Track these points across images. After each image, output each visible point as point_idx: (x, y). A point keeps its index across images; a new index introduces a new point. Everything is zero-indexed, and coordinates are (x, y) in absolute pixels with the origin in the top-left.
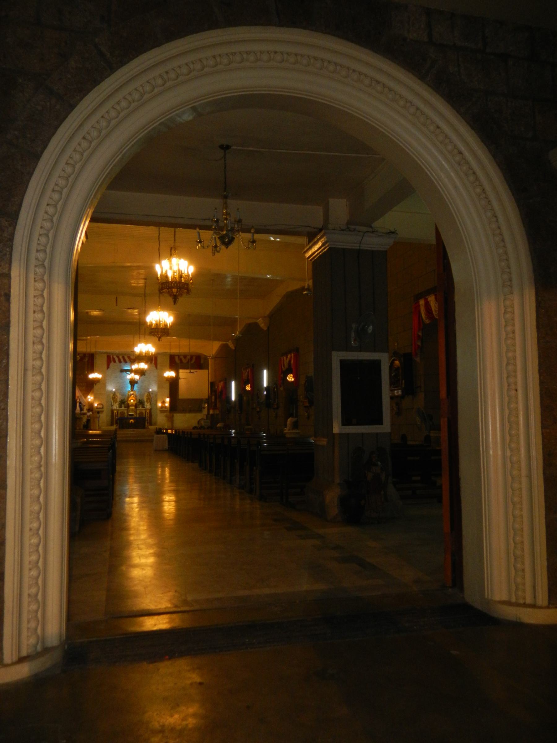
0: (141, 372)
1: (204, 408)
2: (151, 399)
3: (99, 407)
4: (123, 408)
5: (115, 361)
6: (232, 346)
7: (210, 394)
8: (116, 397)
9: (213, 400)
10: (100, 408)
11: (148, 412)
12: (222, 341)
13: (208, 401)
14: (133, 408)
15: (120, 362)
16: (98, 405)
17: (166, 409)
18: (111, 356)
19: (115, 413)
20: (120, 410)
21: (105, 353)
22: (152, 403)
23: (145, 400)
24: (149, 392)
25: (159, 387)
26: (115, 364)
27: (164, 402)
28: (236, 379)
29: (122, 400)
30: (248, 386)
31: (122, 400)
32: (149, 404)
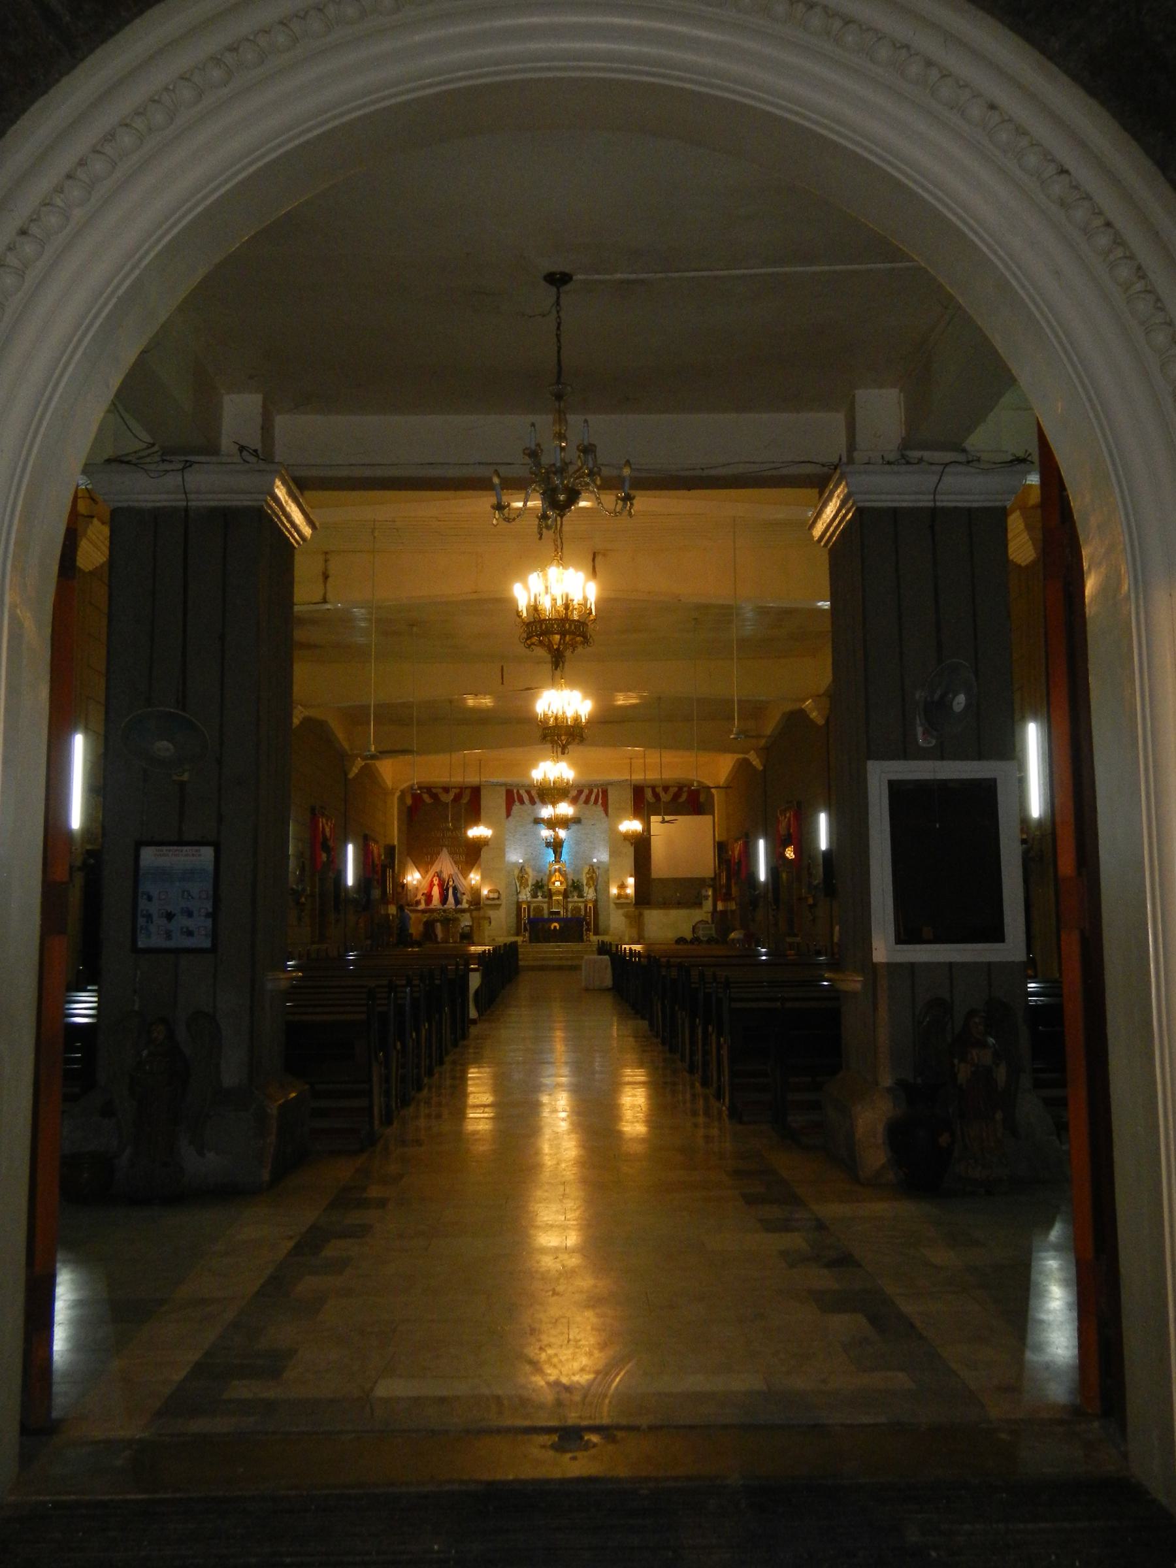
0: (564, 822)
1: (707, 897)
2: (597, 879)
3: (492, 896)
5: (522, 802)
6: (756, 762)
7: (717, 869)
8: (526, 876)
9: (724, 881)
12: (738, 753)
13: (714, 882)
16: (489, 891)
17: (629, 901)
18: (515, 791)
19: (525, 908)
20: (535, 902)
21: (501, 785)
22: (598, 888)
23: (585, 883)
24: (592, 865)
25: (613, 853)
26: (524, 807)
27: (622, 886)
28: (766, 836)
29: (537, 882)
30: (790, 849)
31: (537, 881)
32: (591, 890)
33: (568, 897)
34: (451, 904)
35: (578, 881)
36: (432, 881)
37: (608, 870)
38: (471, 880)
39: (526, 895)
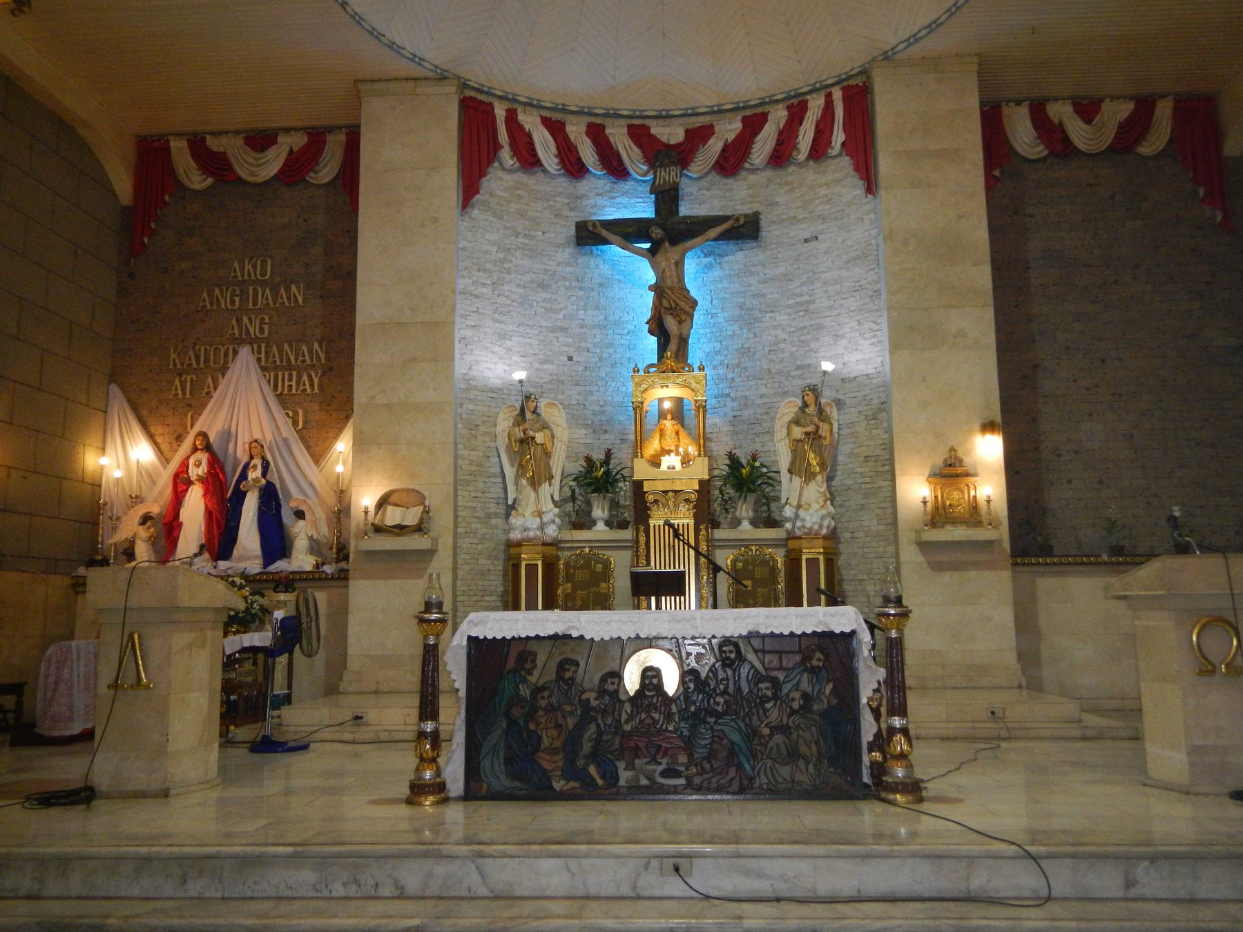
2: (835, 447)
3: (393, 516)
4: (600, 530)
5: (529, 159)
8: (539, 437)
10: (400, 529)
11: (813, 563)
14: (684, 518)
15: (573, 167)
18: (500, 112)
21: (442, 78)
31: (588, 459)
32: (815, 491)
33: (715, 525)
34: (249, 558)
35: (754, 458)
36: (184, 466)
37: (884, 407)
38: (337, 462)
39: (540, 514)
